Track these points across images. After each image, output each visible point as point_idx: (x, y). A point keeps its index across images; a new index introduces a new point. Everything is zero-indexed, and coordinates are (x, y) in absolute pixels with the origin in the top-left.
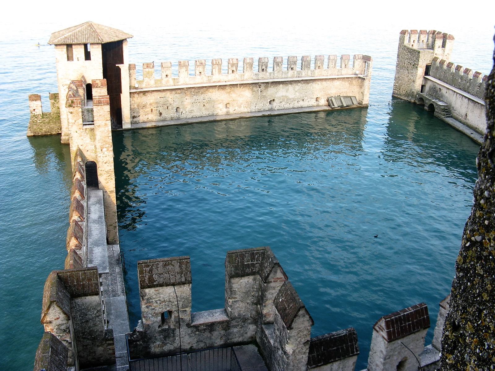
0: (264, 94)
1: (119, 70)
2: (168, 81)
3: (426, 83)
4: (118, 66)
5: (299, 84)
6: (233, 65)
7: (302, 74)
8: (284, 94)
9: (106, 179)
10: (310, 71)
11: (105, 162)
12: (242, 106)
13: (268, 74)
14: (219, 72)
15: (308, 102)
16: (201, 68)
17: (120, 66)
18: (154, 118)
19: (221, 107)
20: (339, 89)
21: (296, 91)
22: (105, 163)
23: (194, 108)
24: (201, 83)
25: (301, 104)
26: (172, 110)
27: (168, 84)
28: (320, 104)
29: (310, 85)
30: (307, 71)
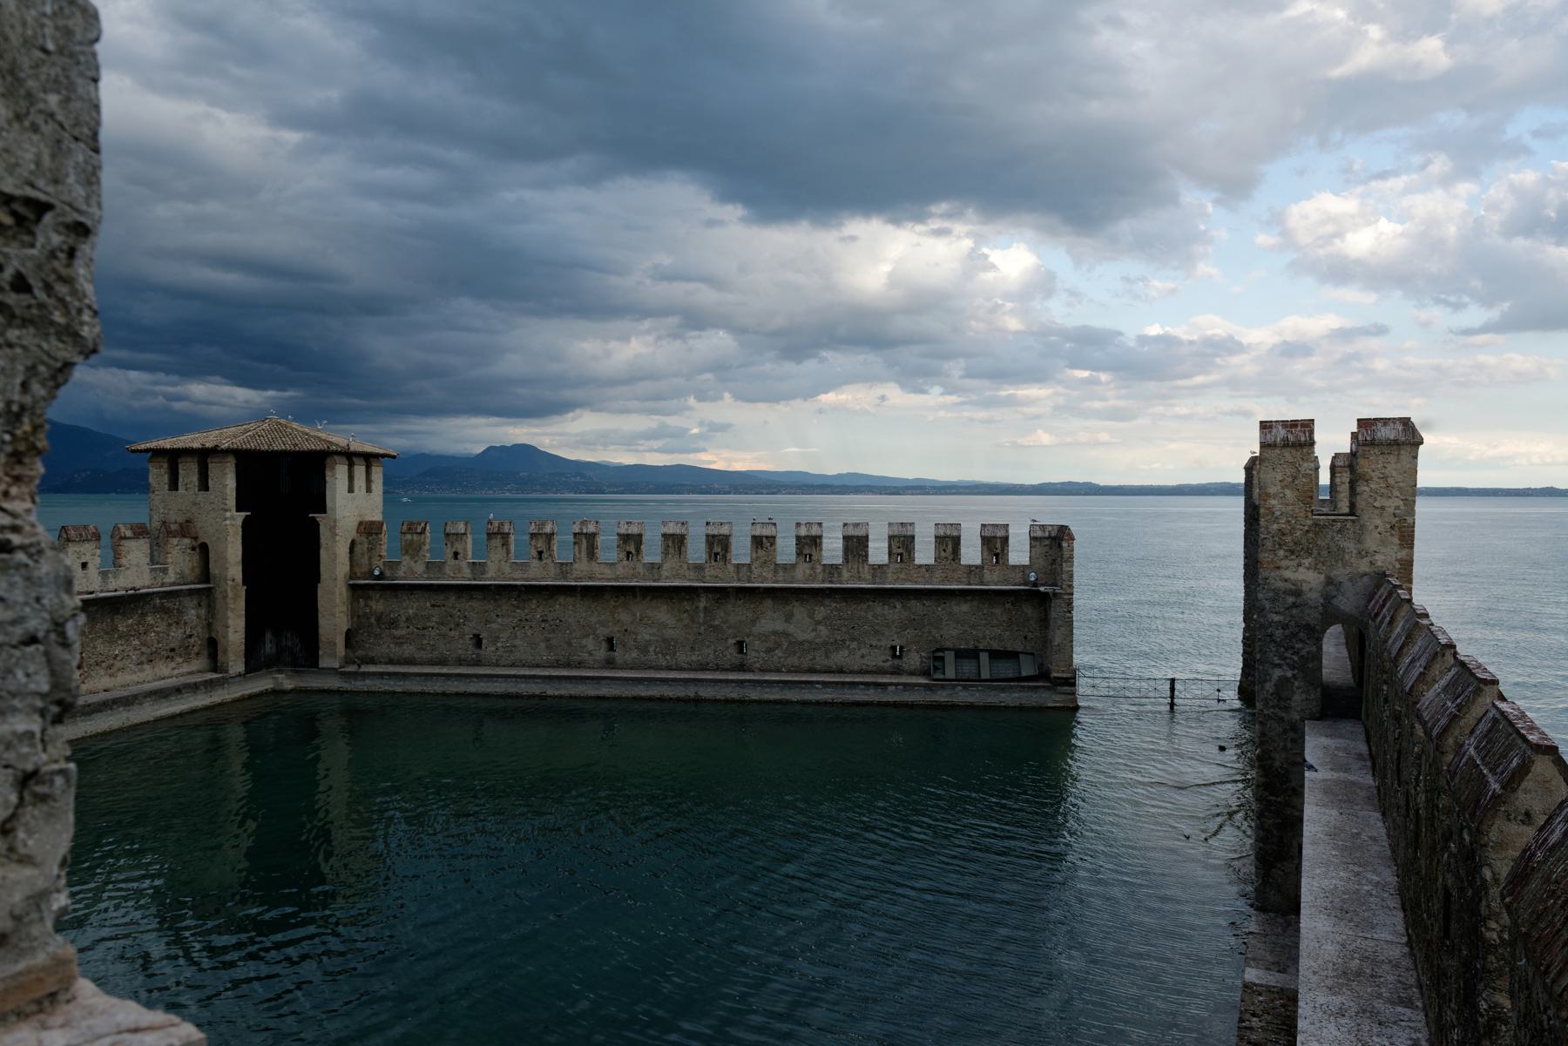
0: (717, 623)
1: (316, 525)
2: (460, 569)
5: (827, 602)
6: (625, 538)
7: (840, 575)
8: (780, 626)
10: (866, 567)
12: (651, 649)
13: (731, 568)
15: (863, 657)
18: (416, 656)
19: (591, 647)
20: (973, 627)
21: (819, 623)
23: (518, 642)
24: (543, 579)
26: (461, 641)
27: (460, 575)
28: (906, 667)
29: (864, 606)
30: (856, 566)
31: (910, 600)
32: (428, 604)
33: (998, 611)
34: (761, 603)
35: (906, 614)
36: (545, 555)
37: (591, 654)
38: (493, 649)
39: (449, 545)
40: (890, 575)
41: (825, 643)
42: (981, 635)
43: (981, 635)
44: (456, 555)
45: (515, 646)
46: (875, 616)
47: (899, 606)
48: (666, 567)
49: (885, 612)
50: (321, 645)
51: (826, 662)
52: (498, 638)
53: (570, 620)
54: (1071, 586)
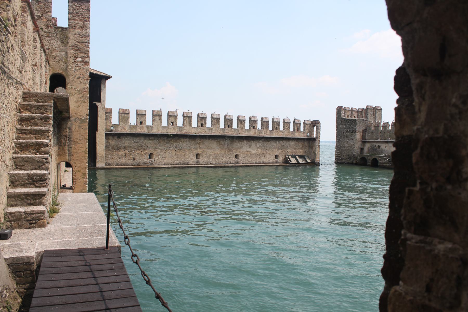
0: (230, 148)
1: (97, 107)
3: (364, 146)
4: (95, 104)
5: (260, 141)
6: (202, 118)
9: (77, 102)
11: (77, 77)
12: (211, 157)
13: (233, 130)
14: (189, 124)
16: (173, 118)
17: (98, 104)
18: (128, 162)
21: (258, 148)
22: (78, 78)
23: (167, 156)
25: (263, 159)
29: (269, 142)
30: (266, 130)
31: (280, 141)
32: (133, 142)
33: (300, 144)
34: (243, 141)
35: (279, 145)
36: (174, 124)
37: (191, 160)
38: (157, 158)
39: (139, 119)
40: (274, 133)
41: (260, 154)
42: (296, 151)
43: (296, 151)
44: (141, 123)
45: (165, 157)
46: (272, 146)
47: (278, 143)
48: (214, 129)
49: (275, 144)
50: (97, 157)
51: (259, 160)
52: (159, 154)
53: (185, 147)
54: (320, 137)
